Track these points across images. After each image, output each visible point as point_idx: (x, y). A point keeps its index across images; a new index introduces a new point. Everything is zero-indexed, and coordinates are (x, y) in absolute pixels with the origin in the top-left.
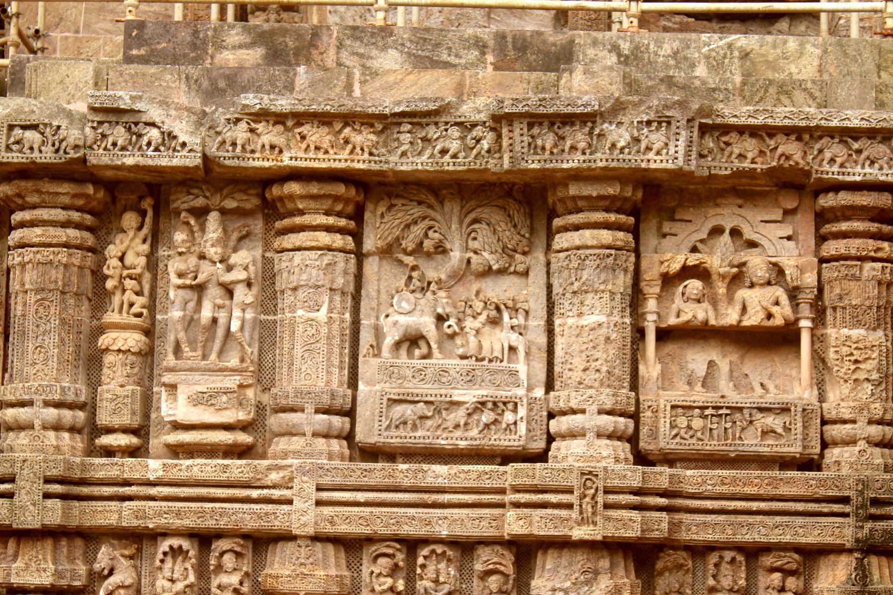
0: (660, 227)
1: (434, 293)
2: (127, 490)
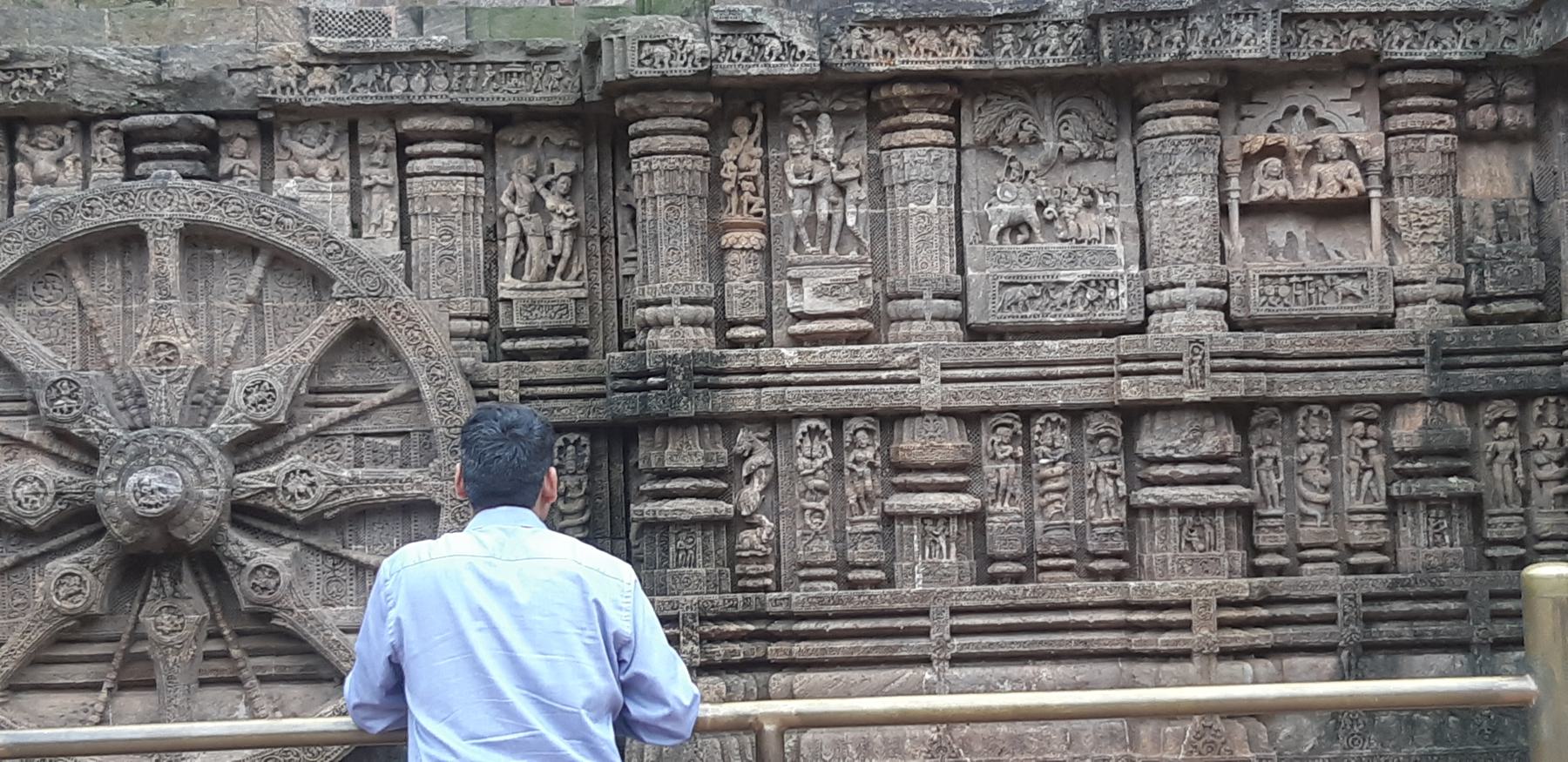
0: (1238, 110)
1: (1033, 181)
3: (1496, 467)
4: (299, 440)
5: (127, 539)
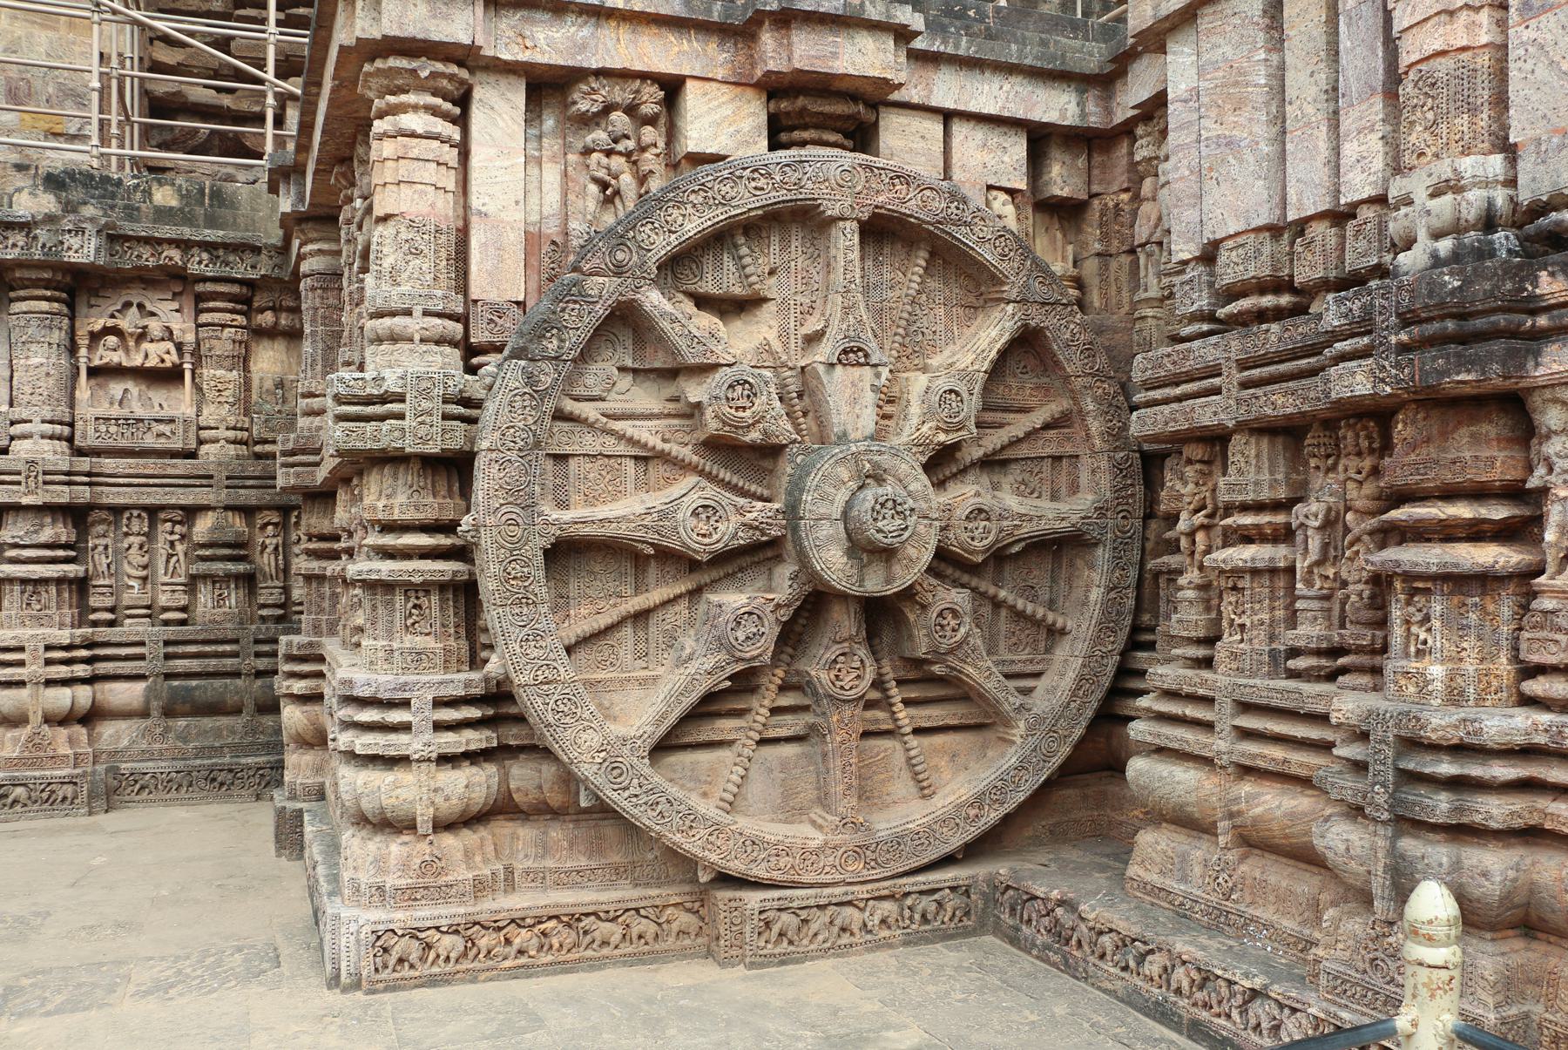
3: (265, 555)
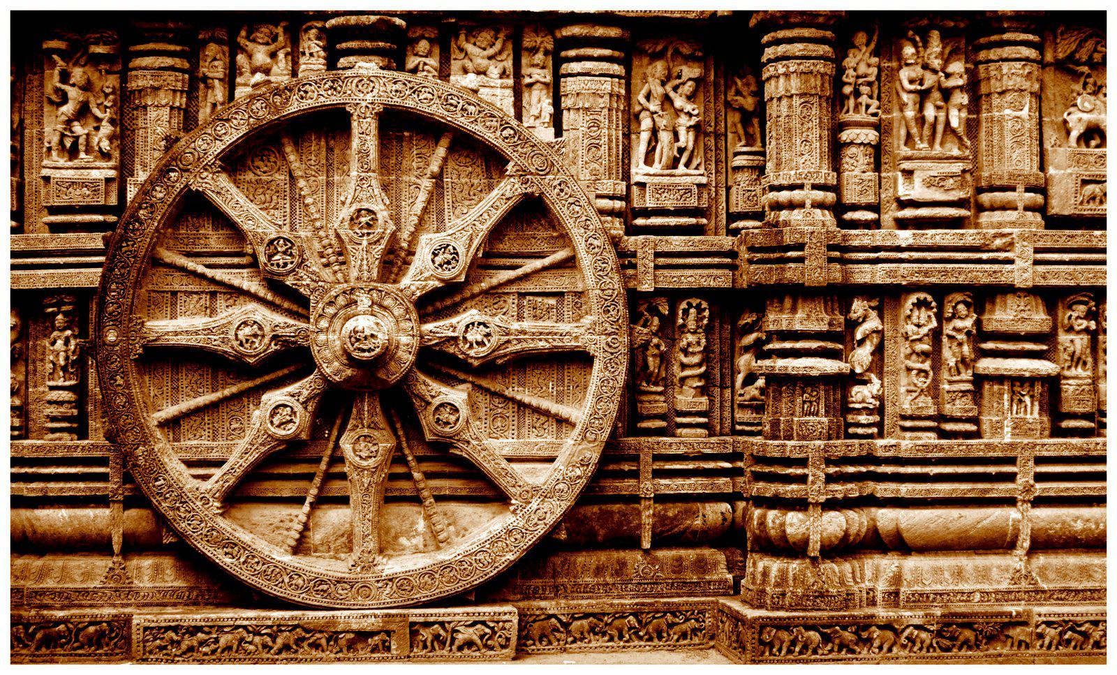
2: (882, 255)
4: (473, 296)
5: (337, 378)
